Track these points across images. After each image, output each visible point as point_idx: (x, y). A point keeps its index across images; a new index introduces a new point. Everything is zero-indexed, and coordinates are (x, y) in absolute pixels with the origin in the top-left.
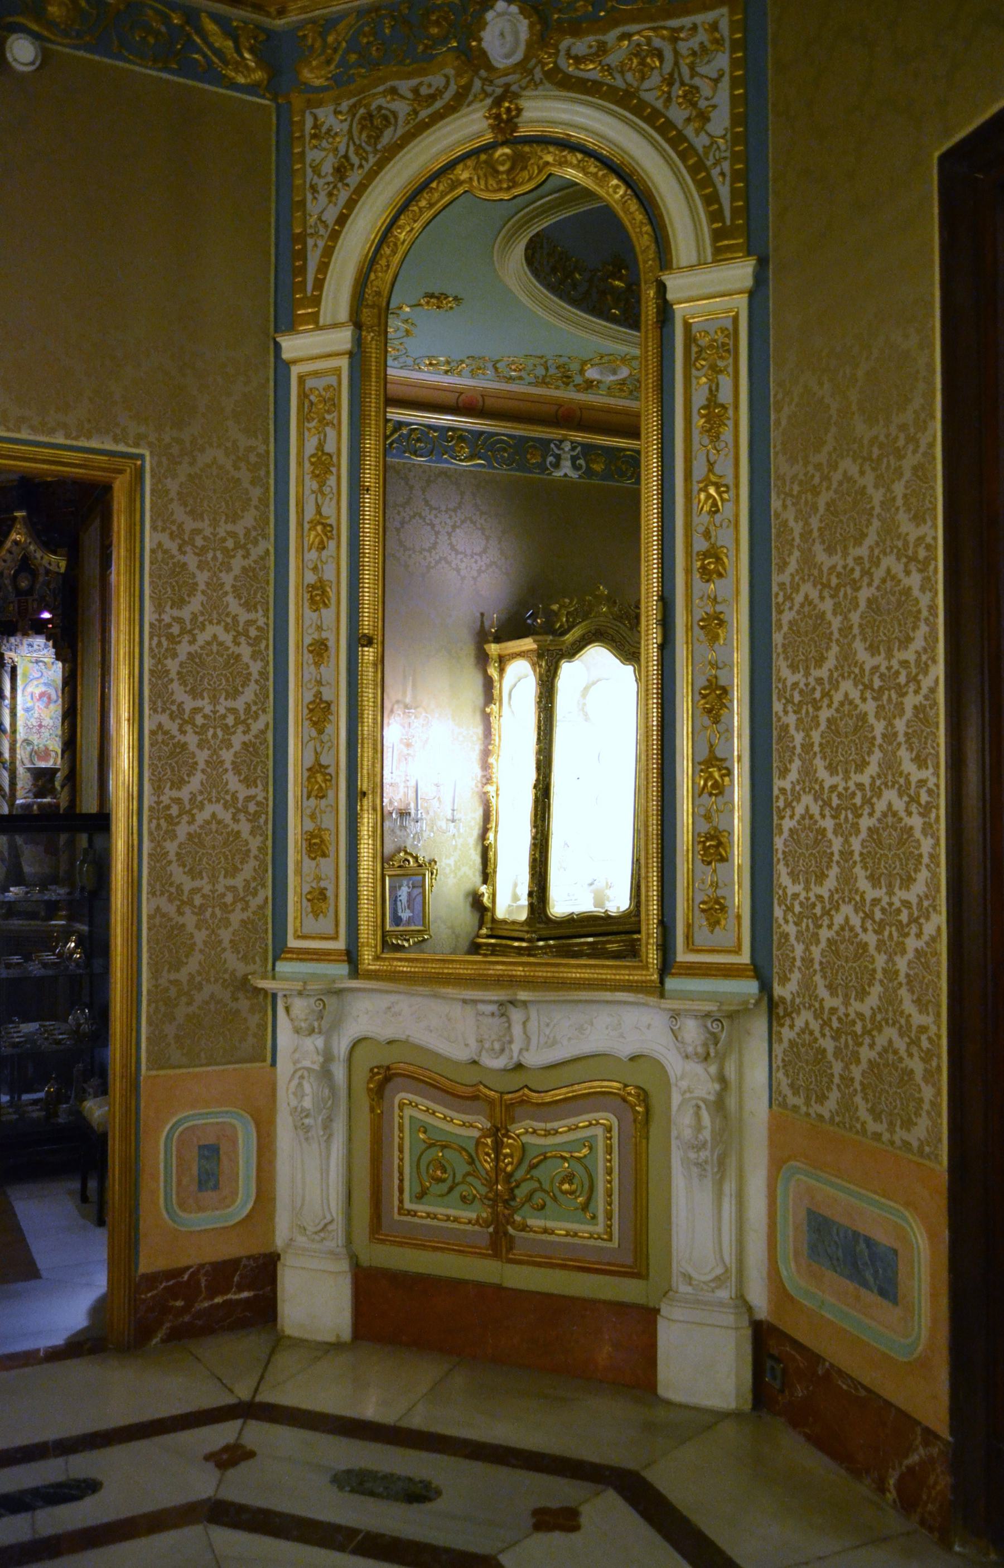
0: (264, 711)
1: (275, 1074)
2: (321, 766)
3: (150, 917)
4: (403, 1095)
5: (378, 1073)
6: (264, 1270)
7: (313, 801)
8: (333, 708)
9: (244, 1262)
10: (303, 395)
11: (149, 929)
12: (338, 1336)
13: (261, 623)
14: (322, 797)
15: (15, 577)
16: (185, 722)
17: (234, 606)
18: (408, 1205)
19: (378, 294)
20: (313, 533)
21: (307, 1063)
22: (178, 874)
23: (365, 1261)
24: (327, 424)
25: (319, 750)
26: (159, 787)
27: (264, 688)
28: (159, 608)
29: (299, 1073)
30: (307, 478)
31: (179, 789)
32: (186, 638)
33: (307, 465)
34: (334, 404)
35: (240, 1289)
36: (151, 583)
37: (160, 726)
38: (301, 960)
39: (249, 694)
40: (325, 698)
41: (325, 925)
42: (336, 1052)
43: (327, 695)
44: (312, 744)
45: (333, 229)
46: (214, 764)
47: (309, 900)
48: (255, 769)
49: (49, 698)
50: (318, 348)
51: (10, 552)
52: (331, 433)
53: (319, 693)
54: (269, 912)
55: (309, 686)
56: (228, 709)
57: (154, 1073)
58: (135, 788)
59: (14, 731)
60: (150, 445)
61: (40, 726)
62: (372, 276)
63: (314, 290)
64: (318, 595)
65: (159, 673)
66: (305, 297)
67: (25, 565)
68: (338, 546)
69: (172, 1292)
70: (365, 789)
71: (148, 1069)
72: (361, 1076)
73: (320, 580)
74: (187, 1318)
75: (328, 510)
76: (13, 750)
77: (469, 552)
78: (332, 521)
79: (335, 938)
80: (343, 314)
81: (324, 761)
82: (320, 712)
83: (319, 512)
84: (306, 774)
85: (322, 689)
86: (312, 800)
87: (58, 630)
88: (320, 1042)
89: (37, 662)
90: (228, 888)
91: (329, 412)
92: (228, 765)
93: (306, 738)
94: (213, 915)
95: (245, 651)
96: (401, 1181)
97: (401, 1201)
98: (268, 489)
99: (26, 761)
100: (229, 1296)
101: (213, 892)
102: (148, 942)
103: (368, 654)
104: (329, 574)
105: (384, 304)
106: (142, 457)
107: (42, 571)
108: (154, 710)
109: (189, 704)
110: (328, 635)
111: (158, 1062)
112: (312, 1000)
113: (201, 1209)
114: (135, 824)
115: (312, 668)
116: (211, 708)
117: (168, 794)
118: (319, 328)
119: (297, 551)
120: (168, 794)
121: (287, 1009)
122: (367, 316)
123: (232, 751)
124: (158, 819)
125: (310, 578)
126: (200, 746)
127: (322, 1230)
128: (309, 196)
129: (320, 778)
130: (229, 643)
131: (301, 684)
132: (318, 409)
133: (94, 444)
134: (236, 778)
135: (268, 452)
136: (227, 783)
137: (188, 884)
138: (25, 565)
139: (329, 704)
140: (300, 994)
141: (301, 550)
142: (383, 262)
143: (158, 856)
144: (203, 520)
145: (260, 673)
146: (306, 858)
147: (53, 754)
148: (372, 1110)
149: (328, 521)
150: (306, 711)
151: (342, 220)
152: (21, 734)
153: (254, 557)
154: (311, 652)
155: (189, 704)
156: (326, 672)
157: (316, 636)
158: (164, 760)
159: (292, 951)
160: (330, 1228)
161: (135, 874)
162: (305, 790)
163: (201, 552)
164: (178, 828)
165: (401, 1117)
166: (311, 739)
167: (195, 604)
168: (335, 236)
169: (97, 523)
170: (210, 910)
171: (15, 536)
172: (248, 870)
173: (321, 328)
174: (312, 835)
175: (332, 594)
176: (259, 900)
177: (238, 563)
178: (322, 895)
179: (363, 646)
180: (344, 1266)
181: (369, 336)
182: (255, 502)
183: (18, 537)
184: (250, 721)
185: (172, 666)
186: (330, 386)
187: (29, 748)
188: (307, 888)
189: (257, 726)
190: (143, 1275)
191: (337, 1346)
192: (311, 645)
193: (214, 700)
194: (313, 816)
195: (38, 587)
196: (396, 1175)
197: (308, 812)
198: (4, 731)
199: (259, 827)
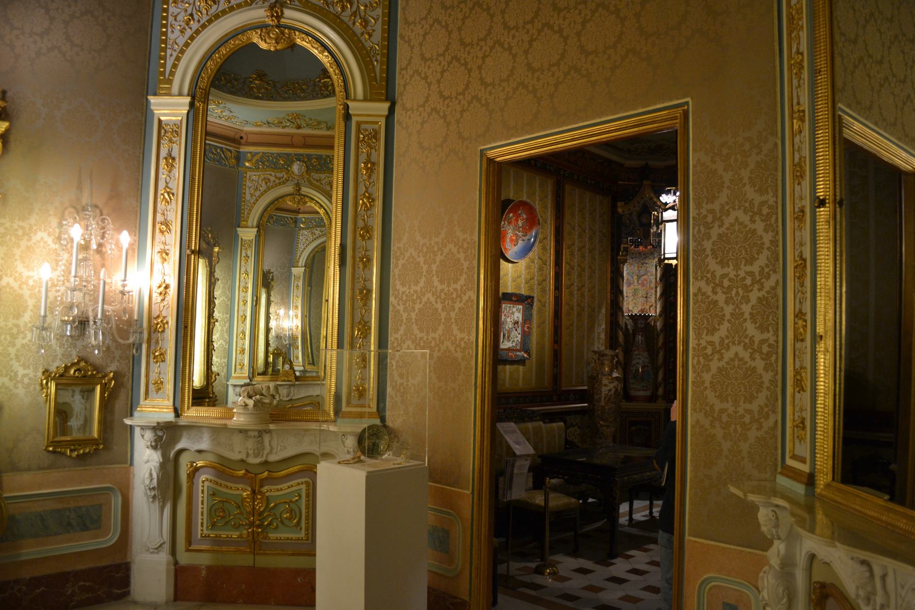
3: (693, 427)
11: (692, 435)
13: (771, 202)
16: (717, 285)
22: (711, 396)
26: (699, 333)
31: (713, 334)
46: (737, 315)
48: (768, 318)
56: (747, 273)
65: (700, 251)
92: (747, 316)
101: (736, 412)
108: (696, 279)
109: (719, 271)
116: (735, 273)
120: (706, 338)
123: (750, 305)
124: (698, 356)
126: (727, 302)
130: (747, 222)
134: (753, 325)
136: (746, 330)
137: (718, 406)
145: (771, 242)
155: (719, 271)
164: (711, 363)
172: (762, 398)
184: (763, 280)
185: (708, 245)
189: (769, 284)
193: (737, 267)
199: (771, 364)
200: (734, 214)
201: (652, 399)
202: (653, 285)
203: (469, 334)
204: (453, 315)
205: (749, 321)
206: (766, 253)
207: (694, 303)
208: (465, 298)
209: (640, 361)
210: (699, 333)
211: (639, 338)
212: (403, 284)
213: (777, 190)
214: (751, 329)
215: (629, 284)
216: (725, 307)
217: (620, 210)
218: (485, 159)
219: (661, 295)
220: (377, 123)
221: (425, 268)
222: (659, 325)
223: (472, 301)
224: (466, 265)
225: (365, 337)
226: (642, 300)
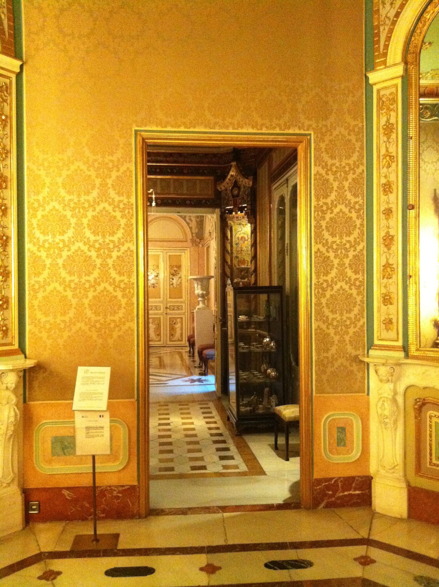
0: (362, 241)
1: (369, 399)
2: (389, 264)
4: (431, 412)
5: (419, 401)
6: (366, 483)
7: (385, 280)
8: (395, 238)
9: (357, 478)
10: (379, 99)
11: (315, 335)
12: (401, 516)
13: (361, 202)
14: (390, 278)
17: (349, 195)
18: (434, 461)
19: (416, 47)
20: (385, 160)
21: (385, 395)
22: (327, 312)
23: (413, 485)
24: (391, 110)
25: (388, 257)
26: (318, 275)
27: (362, 231)
28: (318, 199)
29: (383, 399)
30: (382, 135)
32: (329, 211)
33: (381, 130)
34: (394, 101)
35: (355, 490)
36: (315, 188)
37: (318, 249)
38: (381, 350)
39: (356, 234)
40: (391, 234)
41: (392, 334)
42: (398, 390)
43: (392, 232)
44: (385, 254)
45: (393, 20)
47: (384, 324)
50: (386, 77)
51: (230, 180)
52: (393, 114)
53: (388, 233)
54: (365, 328)
55: (383, 229)
57: (318, 395)
58: (309, 276)
59: (232, 253)
60: (314, 129)
62: (413, 39)
63: (384, 49)
64: (387, 188)
65: (318, 227)
66: (380, 54)
67: (236, 185)
68: (397, 165)
69: (328, 488)
70: (411, 274)
71: (316, 393)
72: (411, 402)
73: (388, 181)
74: (333, 499)
75: (392, 149)
76: (231, 260)
77: (430, 161)
78: (394, 154)
79: (397, 340)
80: (399, 58)
81: (391, 262)
82: (388, 241)
83: (387, 151)
84: (382, 268)
85: (389, 230)
86: (385, 279)
87: (249, 211)
88: (391, 386)
90: (347, 318)
91: (392, 104)
93: (382, 253)
94: (342, 330)
95: (354, 215)
96: (431, 450)
97: (431, 459)
98: (363, 143)
99: (237, 265)
100: (351, 492)
102: (315, 340)
103: (412, 213)
104: (392, 178)
105: (418, 51)
106: (310, 135)
107: (242, 187)
108: (316, 243)
109: (330, 239)
110: (393, 206)
111: (320, 391)
112: (388, 368)
113: (338, 454)
114: (309, 291)
115: (385, 221)
117: (323, 278)
118: (386, 67)
119: (377, 169)
120: (323, 278)
121: (376, 372)
122: (410, 58)
125: (383, 181)
126: (335, 257)
127: (394, 468)
128: (381, 7)
129: (389, 270)
131: (379, 229)
132: (386, 105)
133: (291, 131)
134: (350, 271)
135: (363, 126)
138: (236, 185)
139: (393, 237)
140: (383, 364)
141: (379, 169)
142: (418, 31)
143: (319, 304)
144: (336, 159)
146: (382, 305)
148: (416, 418)
149: (392, 155)
150: (382, 240)
151: (397, 15)
152: (234, 255)
153: (357, 173)
154: (384, 214)
156: (392, 222)
157: (386, 206)
158: (322, 264)
159: (376, 346)
160: (396, 468)
161: (309, 312)
162: (382, 275)
163: (335, 173)
165: (431, 422)
166: (384, 252)
167: (333, 196)
168: (394, 23)
169: (266, 164)
170: (340, 327)
171: (232, 173)
172: (356, 310)
173: (388, 67)
174: (386, 295)
175: (394, 187)
176: (361, 323)
177: (351, 177)
178: (390, 322)
179: (410, 209)
180: (404, 485)
181: (411, 67)
182: (358, 149)
185: (324, 224)
186: (391, 94)
188: (383, 318)
189: (359, 248)
190: (316, 479)
191: (401, 520)
192: (384, 210)
193: (341, 237)
194: (385, 287)
195: (241, 193)
196: (428, 448)
197: (383, 285)
200: (339, 207)
203: (129, 276)
204: (110, 262)
205: (348, 268)
206: (357, 230)
207: (315, 258)
208: (123, 249)
210: (318, 275)
212: (44, 233)
213: (363, 196)
214: (349, 273)
216: (334, 260)
218: (139, 139)
220: (8, 78)
221: (73, 221)
223: (132, 251)
224: (123, 222)
225: (5, 281)
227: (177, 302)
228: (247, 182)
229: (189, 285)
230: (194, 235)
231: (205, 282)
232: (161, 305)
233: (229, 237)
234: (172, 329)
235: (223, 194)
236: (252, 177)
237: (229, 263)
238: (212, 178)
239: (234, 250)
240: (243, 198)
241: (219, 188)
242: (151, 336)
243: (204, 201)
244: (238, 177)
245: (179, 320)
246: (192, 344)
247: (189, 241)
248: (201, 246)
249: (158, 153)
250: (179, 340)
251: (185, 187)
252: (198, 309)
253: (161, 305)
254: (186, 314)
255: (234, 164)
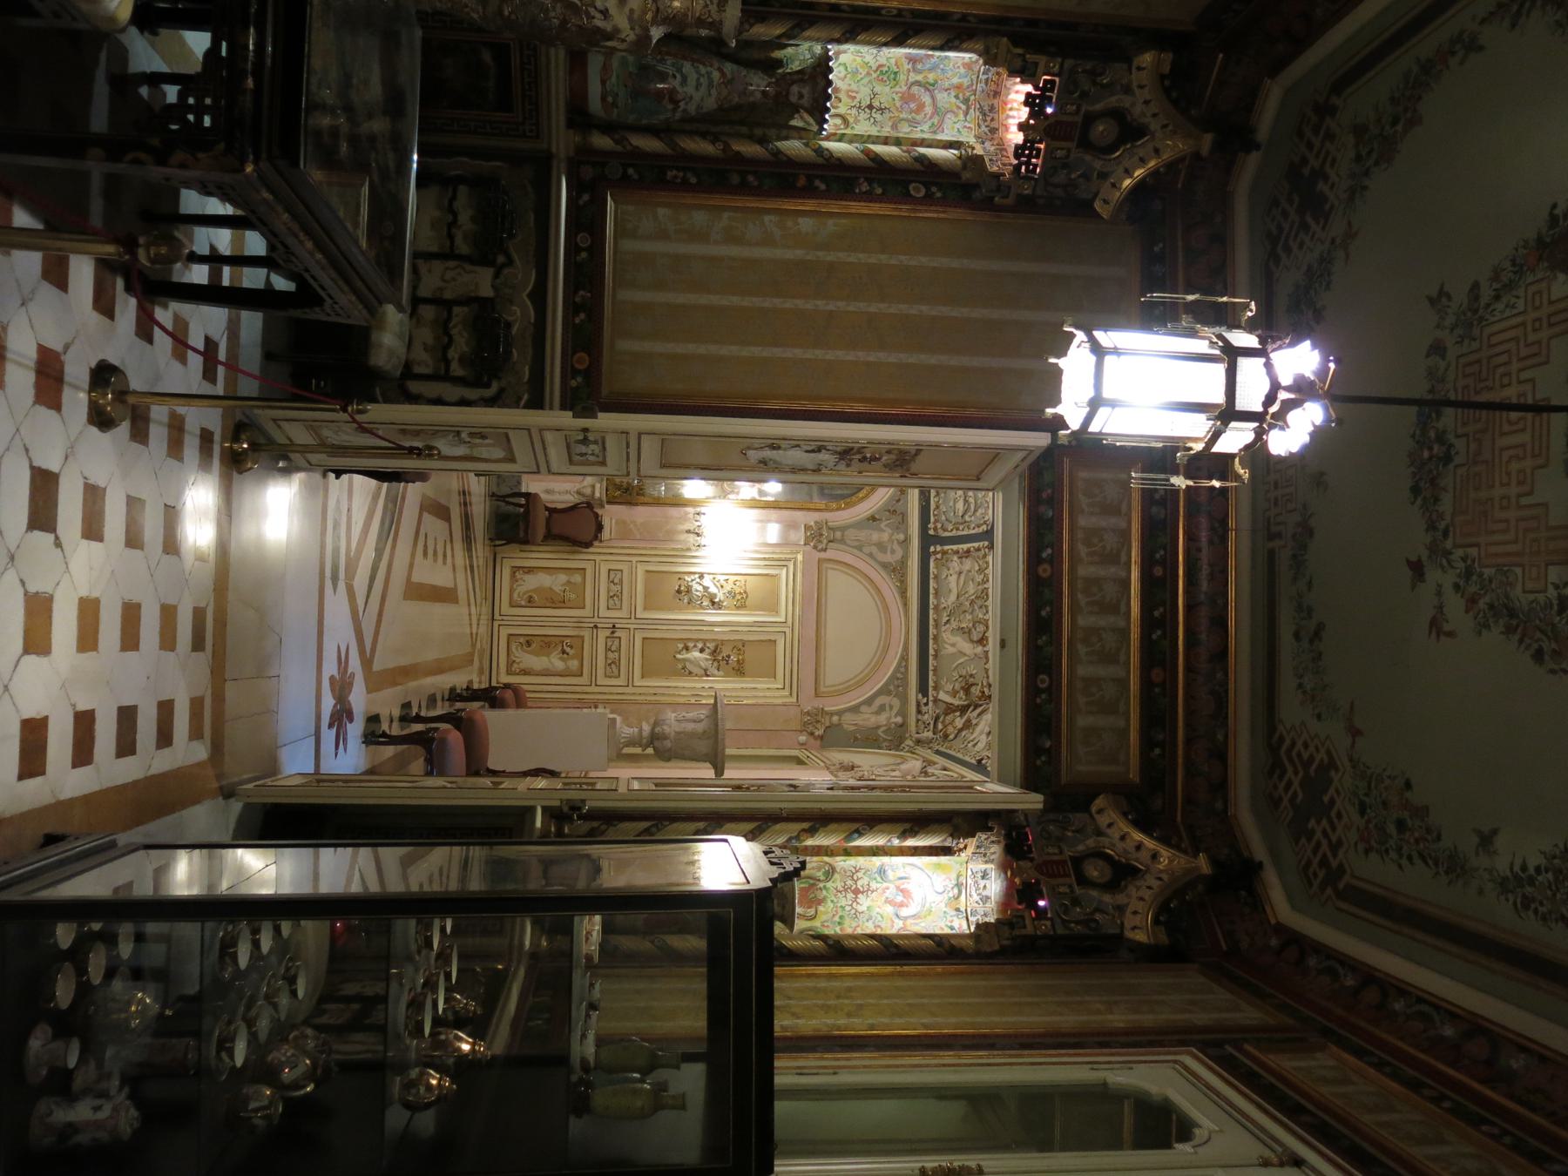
15: (1099, 854)
49: (901, 905)
59: (847, 853)
61: (857, 892)
67: (1123, 873)
89: (958, 885)
107: (1121, 899)
147: (811, 912)
152: (842, 863)
171: (1165, 854)
183: (1164, 862)
187: (820, 875)
195: (1094, 893)
198: (849, 838)
201: (579, 117)
202: (904, 131)
209: (690, 89)
211: (759, 84)
215: (913, 60)
217: (1147, 58)
219: (877, 159)
222: (793, 147)
226: (864, 96)
227: (630, 662)
228: (1139, 922)
229: (682, 700)
230: (835, 719)
231: (703, 747)
232: (624, 613)
233: (911, 842)
234: (547, 644)
235: (1078, 818)
236: (1164, 939)
237: (810, 842)
238: (1134, 775)
239: (861, 861)
240: (1076, 902)
241: (1099, 802)
242: (527, 577)
243: (1048, 744)
244: (1155, 883)
245: (574, 664)
246: (491, 697)
247: (819, 703)
248: (803, 738)
249: (1225, 571)
250: (510, 663)
251: (1101, 671)
252: (614, 720)
253: (624, 613)
254: (593, 689)
255: (1203, 864)
